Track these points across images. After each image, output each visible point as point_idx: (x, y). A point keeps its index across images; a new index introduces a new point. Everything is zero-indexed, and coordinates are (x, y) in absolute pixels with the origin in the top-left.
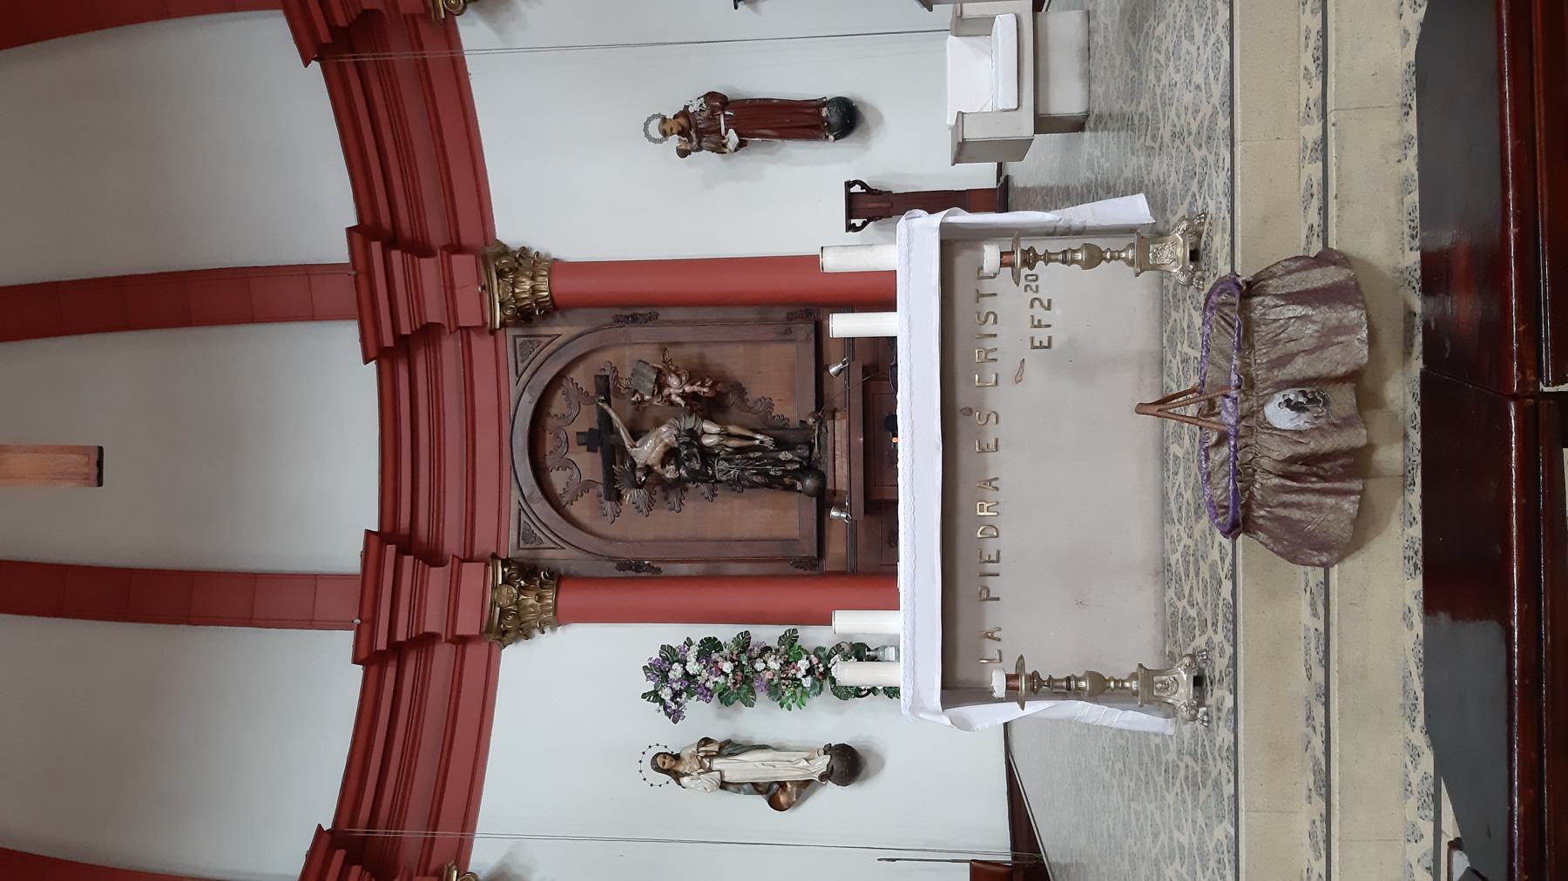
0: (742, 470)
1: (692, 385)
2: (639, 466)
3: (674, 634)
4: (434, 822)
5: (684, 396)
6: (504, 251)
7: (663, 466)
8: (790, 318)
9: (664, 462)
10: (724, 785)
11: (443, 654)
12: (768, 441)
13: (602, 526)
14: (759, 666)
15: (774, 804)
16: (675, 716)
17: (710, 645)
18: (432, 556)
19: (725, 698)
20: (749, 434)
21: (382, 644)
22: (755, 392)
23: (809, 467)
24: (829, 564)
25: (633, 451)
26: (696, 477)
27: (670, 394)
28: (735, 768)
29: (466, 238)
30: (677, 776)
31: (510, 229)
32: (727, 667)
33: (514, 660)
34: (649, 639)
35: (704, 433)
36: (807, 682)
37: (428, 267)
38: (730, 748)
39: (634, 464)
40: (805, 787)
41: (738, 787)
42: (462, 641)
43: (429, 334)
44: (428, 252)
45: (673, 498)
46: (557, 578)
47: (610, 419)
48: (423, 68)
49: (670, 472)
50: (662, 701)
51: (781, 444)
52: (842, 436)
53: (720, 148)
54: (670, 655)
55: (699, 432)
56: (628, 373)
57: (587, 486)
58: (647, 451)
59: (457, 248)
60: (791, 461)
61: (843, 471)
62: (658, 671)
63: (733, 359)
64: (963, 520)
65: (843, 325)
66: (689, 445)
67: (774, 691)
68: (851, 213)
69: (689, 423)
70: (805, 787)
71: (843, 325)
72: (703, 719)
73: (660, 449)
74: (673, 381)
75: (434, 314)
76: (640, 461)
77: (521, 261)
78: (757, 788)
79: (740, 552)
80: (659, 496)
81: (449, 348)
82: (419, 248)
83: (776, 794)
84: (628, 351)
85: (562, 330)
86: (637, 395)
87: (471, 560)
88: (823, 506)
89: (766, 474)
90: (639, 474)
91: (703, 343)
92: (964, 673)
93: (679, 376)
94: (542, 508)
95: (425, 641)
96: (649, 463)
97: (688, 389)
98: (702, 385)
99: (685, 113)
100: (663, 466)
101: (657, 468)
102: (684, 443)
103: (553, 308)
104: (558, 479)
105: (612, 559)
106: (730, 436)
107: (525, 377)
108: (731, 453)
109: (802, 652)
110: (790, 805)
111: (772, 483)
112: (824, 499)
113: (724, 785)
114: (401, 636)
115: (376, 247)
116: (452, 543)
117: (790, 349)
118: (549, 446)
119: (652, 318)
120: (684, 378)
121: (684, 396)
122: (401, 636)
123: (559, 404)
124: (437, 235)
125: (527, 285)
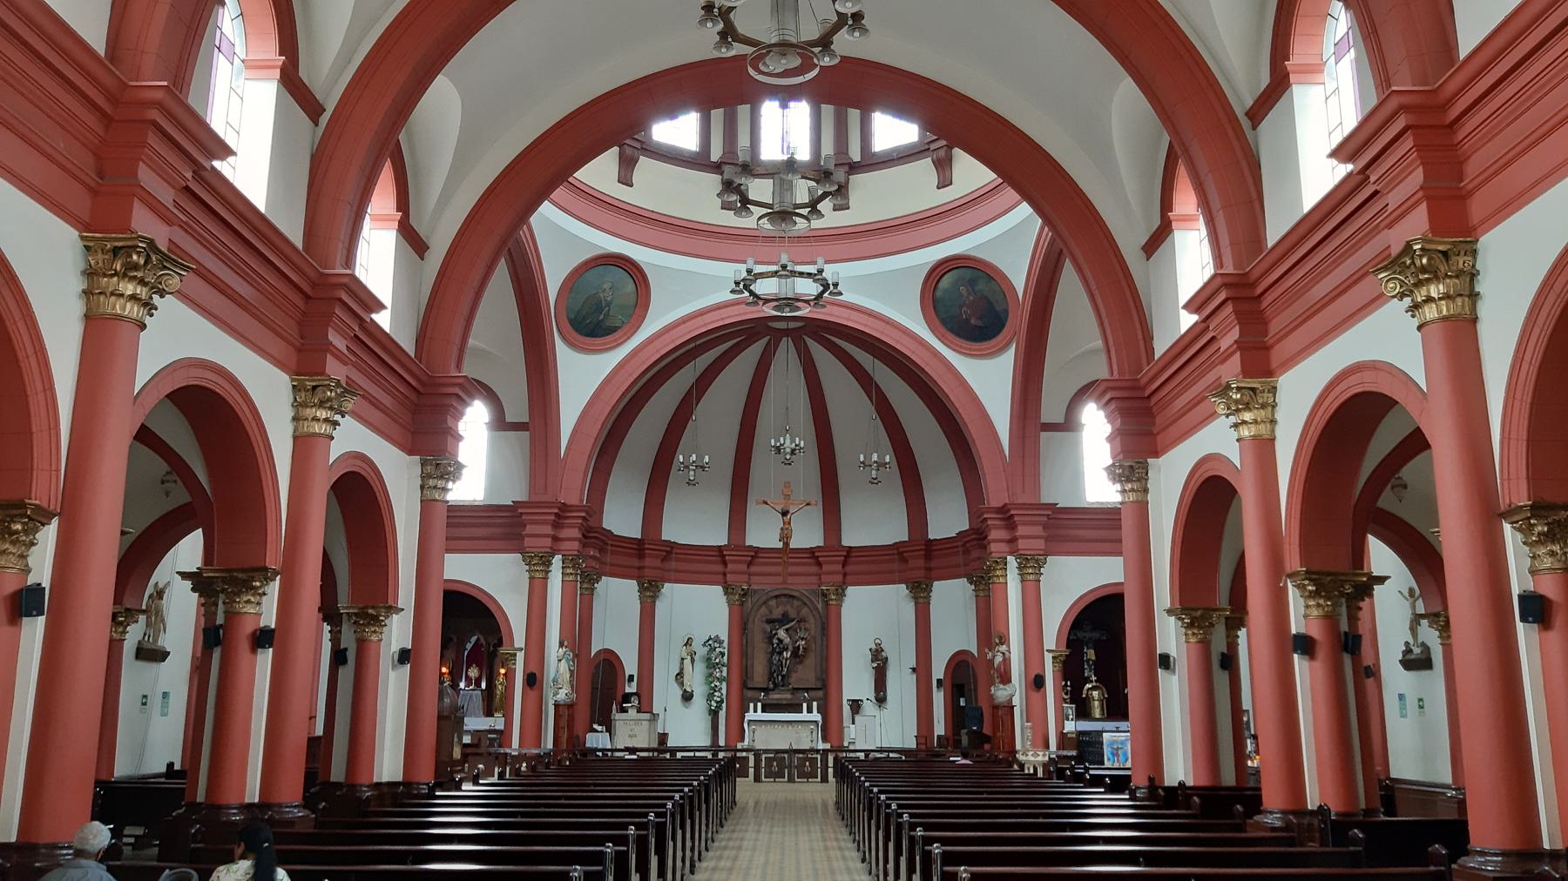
3: (725, 644)
4: (676, 571)
5: (799, 645)
6: (843, 590)
8: (823, 680)
9: (778, 639)
10: (683, 659)
11: (720, 568)
12: (784, 673)
13: (758, 616)
14: (718, 670)
15: (678, 675)
16: (704, 645)
17: (722, 654)
18: (750, 564)
19: (709, 659)
21: (725, 553)
22: (800, 667)
23: (776, 685)
24: (745, 691)
26: (774, 649)
28: (687, 662)
29: (848, 577)
30: (686, 645)
31: (851, 591)
32: (717, 661)
33: (719, 589)
34: (724, 637)
36: (713, 685)
38: (693, 661)
40: (682, 684)
41: (682, 663)
42: (725, 574)
43: (819, 564)
44: (843, 566)
45: (766, 640)
46: (742, 604)
48: (892, 572)
49: (775, 641)
50: (708, 641)
51: (783, 676)
52: (785, 696)
54: (721, 642)
56: (807, 626)
57: (771, 612)
58: (782, 634)
59: (845, 575)
61: (775, 696)
62: (717, 640)
63: (811, 661)
64: (774, 724)
65: (805, 705)
67: (711, 675)
68: (853, 701)
69: (790, 647)
70: (682, 684)
71: (805, 705)
72: (701, 651)
73: (782, 638)
74: (803, 643)
75: (825, 568)
76: (779, 631)
77: (841, 595)
78: (682, 669)
79: (749, 663)
80: (768, 635)
81: (814, 569)
82: (844, 564)
83: (680, 676)
84: (813, 626)
85: (820, 606)
87: (749, 575)
88: (763, 690)
89: (775, 671)
91: (815, 651)
92: (751, 723)
94: (764, 598)
95: (725, 564)
103: (827, 604)
104: (773, 603)
105: (748, 620)
107: (806, 593)
109: (721, 683)
110: (676, 679)
111: (771, 674)
112: (766, 690)
113: (683, 659)
115: (845, 553)
116: (753, 569)
117: (814, 680)
118: (783, 599)
119: (823, 634)
121: (799, 645)
122: (727, 558)
123: (796, 603)
124: (849, 569)
125: (833, 597)
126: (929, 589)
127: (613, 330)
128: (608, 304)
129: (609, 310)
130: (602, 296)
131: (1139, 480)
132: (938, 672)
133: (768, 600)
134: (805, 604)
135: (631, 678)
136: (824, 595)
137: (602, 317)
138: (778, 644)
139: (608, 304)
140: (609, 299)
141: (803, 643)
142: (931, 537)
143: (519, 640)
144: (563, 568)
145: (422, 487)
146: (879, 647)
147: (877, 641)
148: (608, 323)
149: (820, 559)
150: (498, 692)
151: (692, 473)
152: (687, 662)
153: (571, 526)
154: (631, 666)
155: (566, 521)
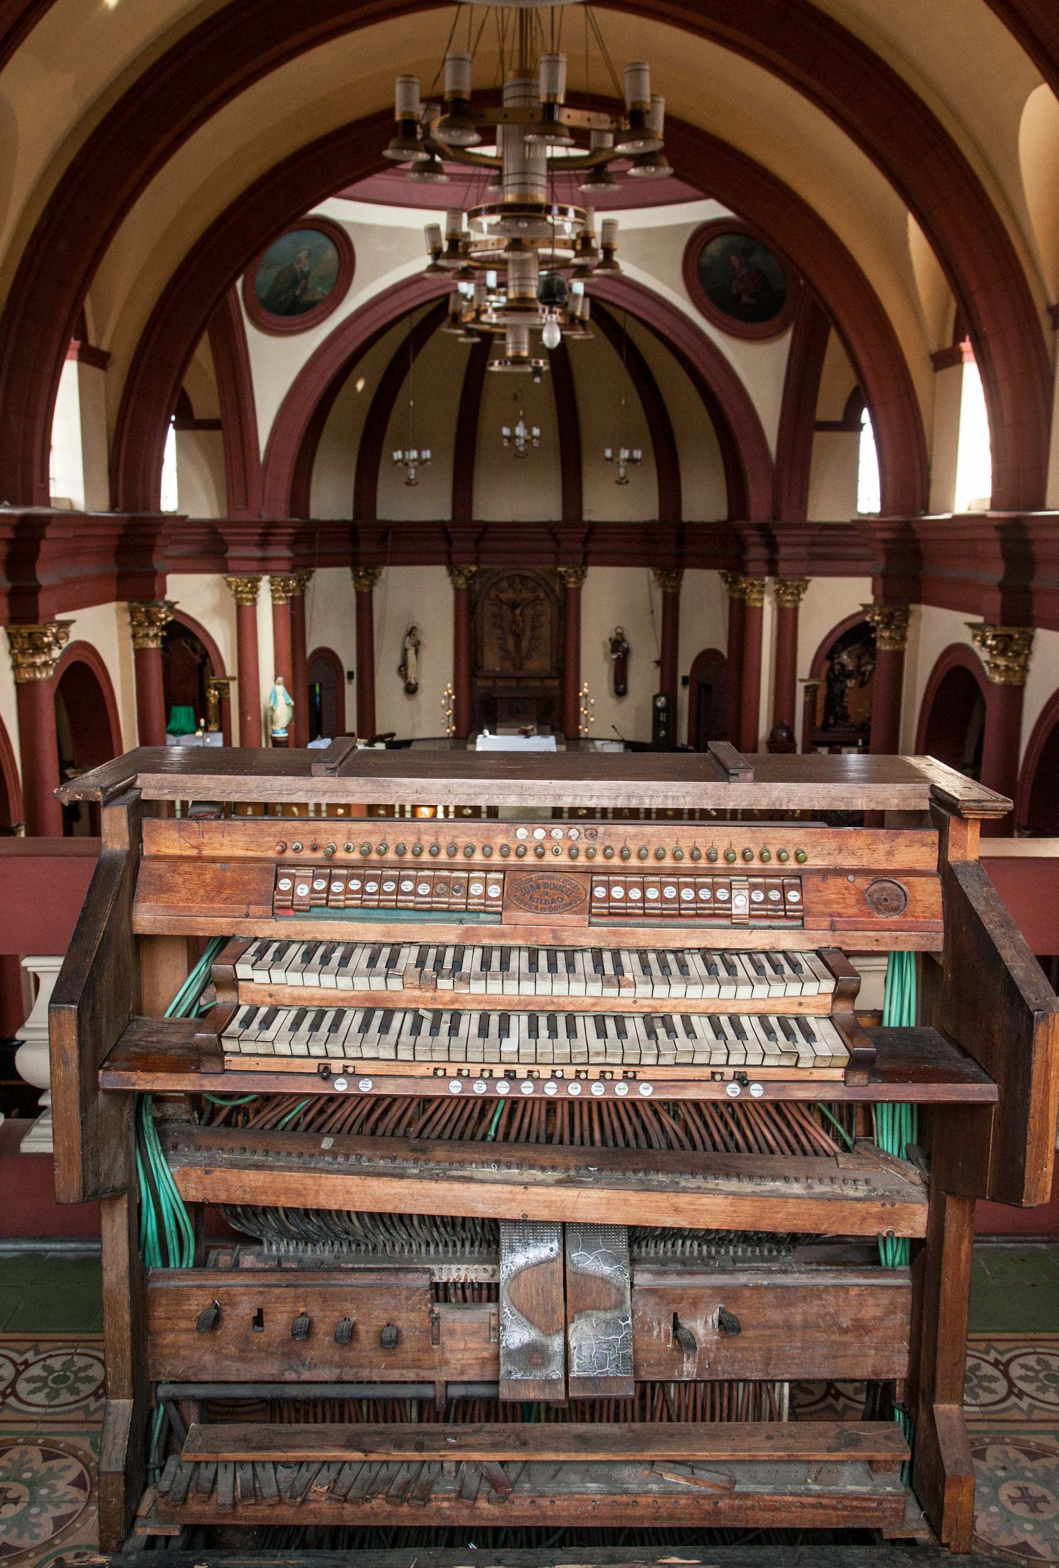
6: (583, 573)
10: (405, 651)
15: (400, 668)
18: (477, 542)
28: (411, 653)
37: (580, 545)
42: (449, 554)
43: (557, 542)
53: (614, 651)
59: (586, 554)
77: (581, 577)
82: (586, 541)
94: (495, 579)
95: (449, 541)
99: (624, 640)
114: (452, 535)
124: (591, 546)
126: (679, 577)
127: (311, 305)
128: (306, 276)
129: (306, 283)
130: (297, 266)
131: (898, 628)
132: (684, 668)
133: (498, 582)
134: (540, 585)
135: (351, 675)
136: (562, 577)
137: (298, 292)
139: (306, 276)
140: (306, 270)
142: (686, 517)
143: (231, 668)
144: (272, 591)
145: (134, 636)
146: (619, 638)
147: (619, 630)
148: (307, 298)
149: (559, 536)
150: (213, 700)
151: (413, 471)
152: (411, 653)
153: (278, 543)
154: (349, 662)
155: (273, 538)
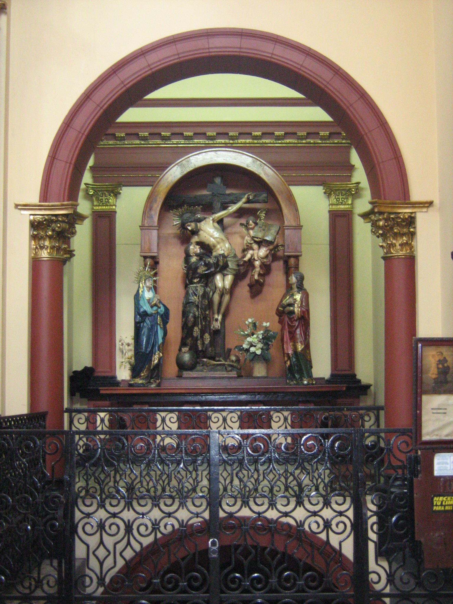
0: (197, 306)
1: (260, 266)
2: (198, 224)
7: (198, 243)
9: (201, 244)
12: (217, 325)
20: (222, 310)
25: (210, 220)
27: (253, 250)
35: (224, 275)
39: (200, 221)
47: (235, 203)
55: (225, 272)
60: (203, 344)
66: (217, 265)
74: (263, 252)
86: (253, 224)
89: (195, 324)
90: (193, 224)
93: (267, 257)
96: (201, 232)
97: (257, 263)
98: (260, 275)
100: (198, 243)
101: (195, 239)
102: (218, 261)
106: (222, 296)
108: (208, 296)
120: (265, 260)
121: (251, 262)
138: (200, 257)
141: (263, 252)
